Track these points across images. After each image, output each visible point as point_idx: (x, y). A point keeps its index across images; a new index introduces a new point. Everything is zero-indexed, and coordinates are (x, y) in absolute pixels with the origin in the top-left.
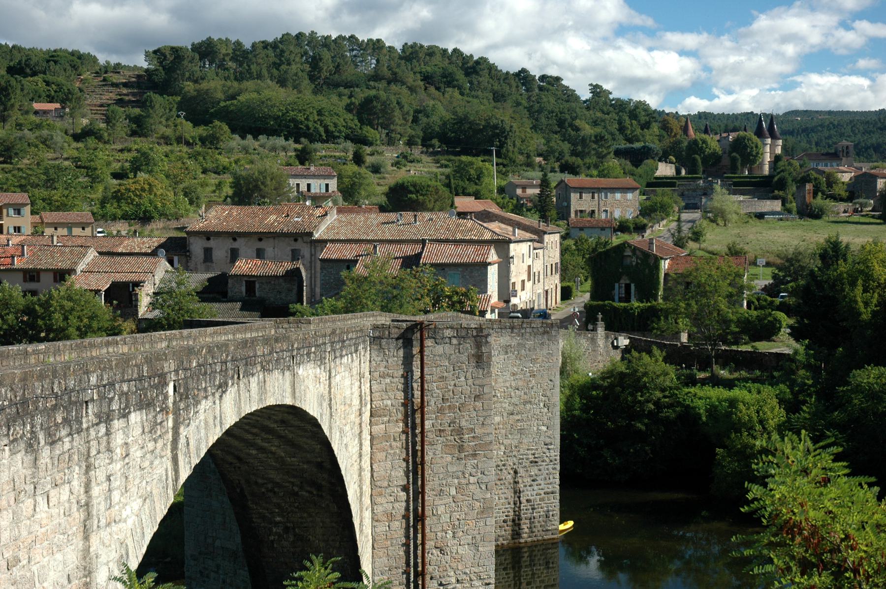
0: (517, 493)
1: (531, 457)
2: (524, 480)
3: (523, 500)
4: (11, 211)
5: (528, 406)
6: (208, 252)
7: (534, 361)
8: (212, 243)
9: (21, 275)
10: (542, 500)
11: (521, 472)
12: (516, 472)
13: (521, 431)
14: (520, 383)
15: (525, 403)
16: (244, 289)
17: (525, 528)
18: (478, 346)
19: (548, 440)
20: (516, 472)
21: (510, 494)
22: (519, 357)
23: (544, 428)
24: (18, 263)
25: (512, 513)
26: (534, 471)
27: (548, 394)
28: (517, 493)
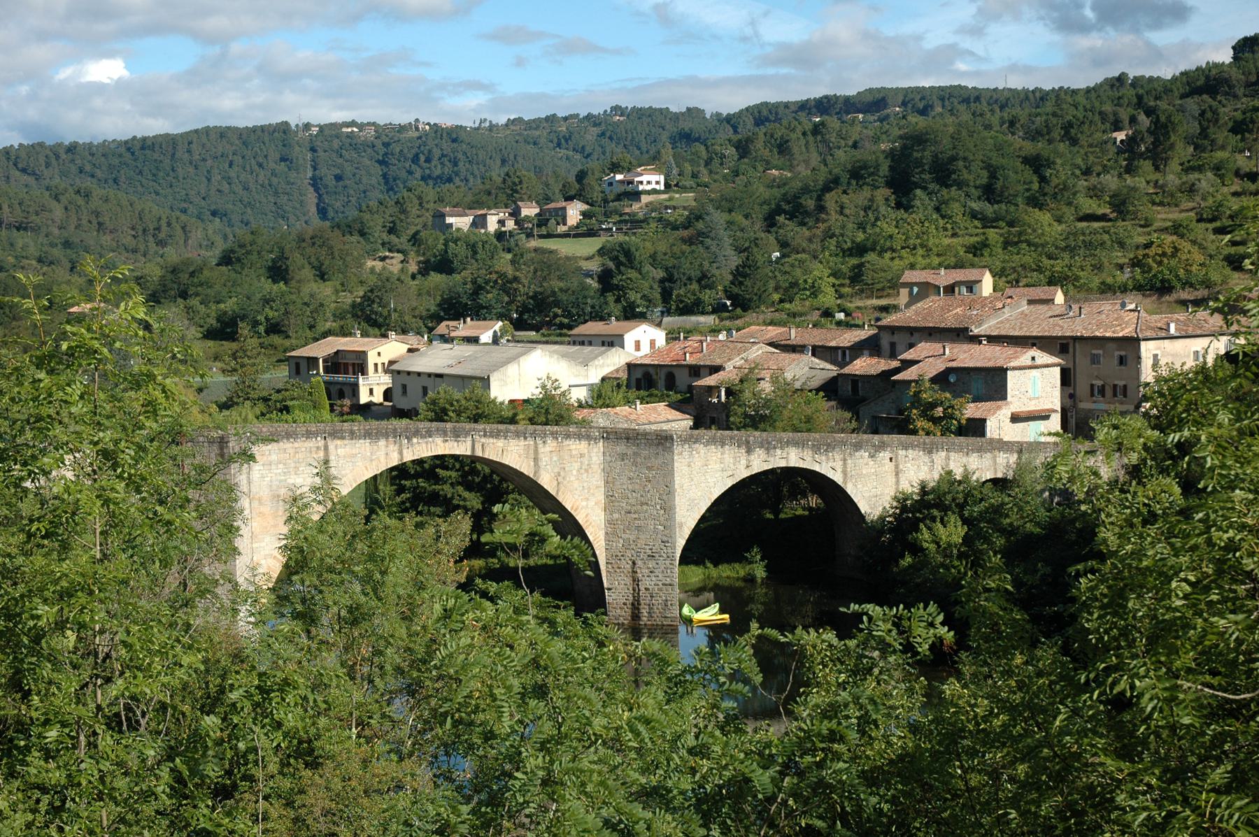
0: (636, 581)
1: (649, 552)
2: (642, 572)
3: (642, 588)
4: (964, 290)
5: (645, 507)
6: (893, 345)
7: (649, 468)
8: (896, 338)
9: (686, 371)
10: (660, 590)
11: (639, 563)
12: (634, 563)
13: (638, 528)
14: (637, 487)
15: (642, 504)
16: (850, 388)
17: (644, 612)
18: (221, 448)
19: (665, 539)
20: (634, 563)
21: (629, 581)
22: (635, 464)
23: (661, 528)
24: (689, 359)
25: (631, 598)
26: (651, 564)
27: (664, 497)
28: (636, 581)
